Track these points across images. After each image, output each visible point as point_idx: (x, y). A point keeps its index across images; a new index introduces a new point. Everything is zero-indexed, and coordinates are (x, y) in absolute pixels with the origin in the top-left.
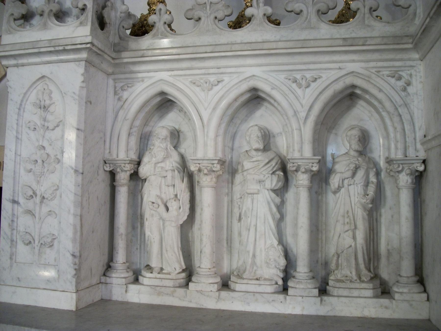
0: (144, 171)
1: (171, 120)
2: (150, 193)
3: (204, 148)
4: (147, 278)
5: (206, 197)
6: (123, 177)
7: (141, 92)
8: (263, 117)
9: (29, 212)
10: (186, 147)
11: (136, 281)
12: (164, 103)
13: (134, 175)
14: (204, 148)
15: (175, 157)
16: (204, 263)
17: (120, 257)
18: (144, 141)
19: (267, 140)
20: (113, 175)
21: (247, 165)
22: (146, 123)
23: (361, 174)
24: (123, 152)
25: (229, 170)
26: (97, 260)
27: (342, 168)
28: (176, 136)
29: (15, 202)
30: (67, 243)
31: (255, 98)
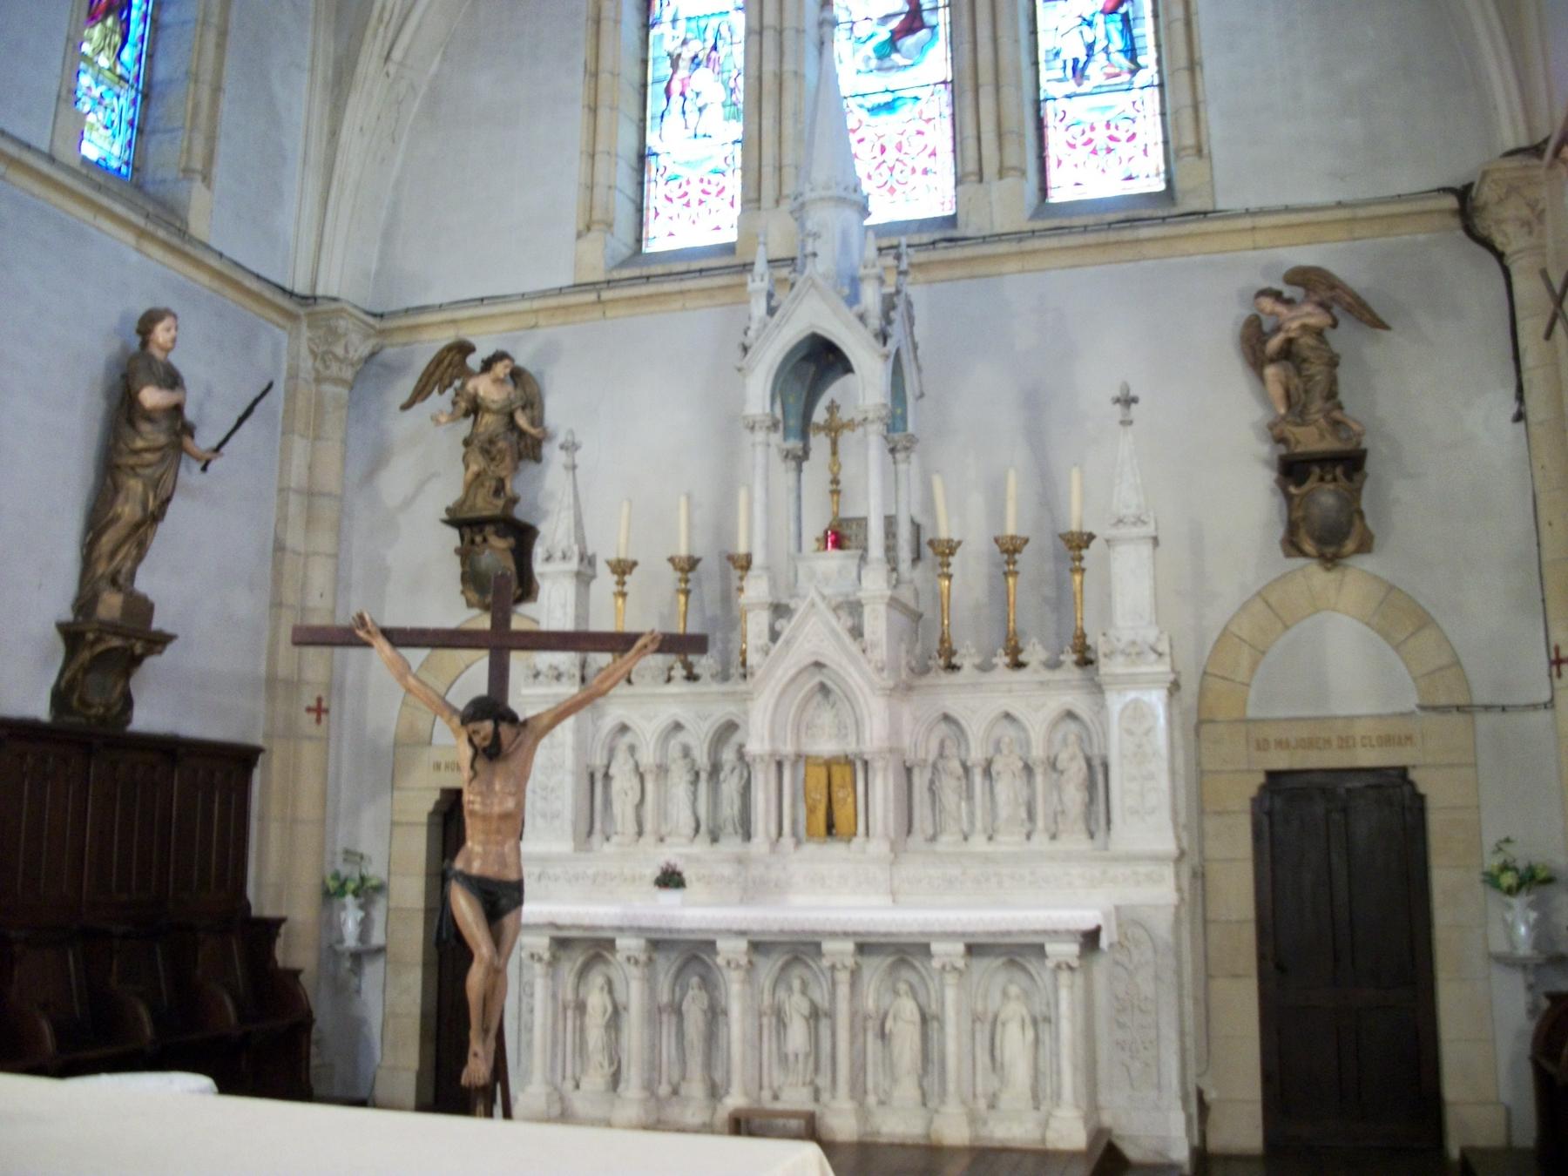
0: (612, 771)
1: (627, 739)
2: (616, 786)
3: (647, 757)
4: (615, 839)
5: (650, 786)
6: (599, 776)
7: (609, 722)
8: (682, 737)
9: (545, 799)
10: (637, 756)
11: (608, 839)
12: (624, 729)
13: (607, 776)
14: (647, 757)
15: (631, 762)
16: (649, 826)
17: (598, 825)
18: (612, 752)
19: (686, 752)
20: (592, 776)
21: (673, 767)
22: (613, 739)
23: (737, 772)
24: (599, 761)
25: (662, 770)
26: (584, 828)
27: (727, 768)
28: (632, 749)
29: (534, 792)
30: (568, 814)
31: (678, 727)
